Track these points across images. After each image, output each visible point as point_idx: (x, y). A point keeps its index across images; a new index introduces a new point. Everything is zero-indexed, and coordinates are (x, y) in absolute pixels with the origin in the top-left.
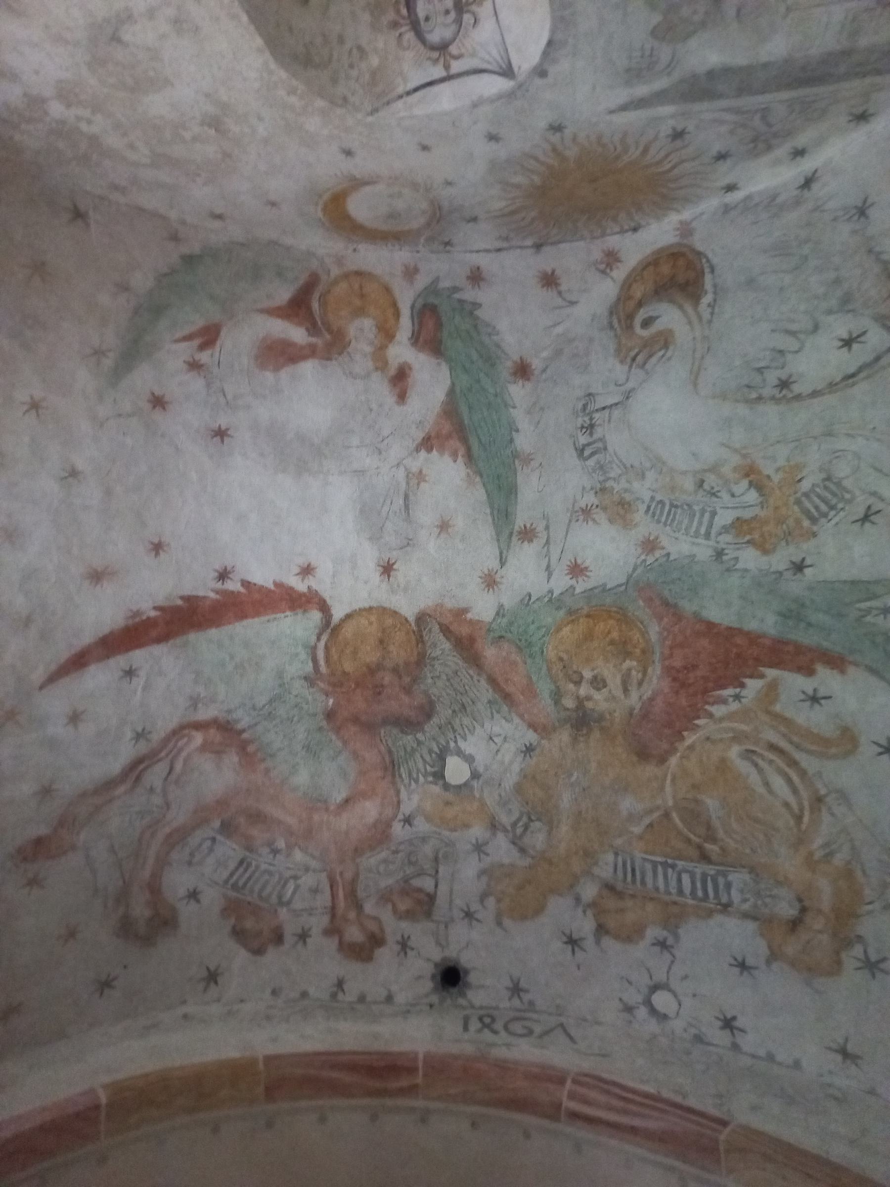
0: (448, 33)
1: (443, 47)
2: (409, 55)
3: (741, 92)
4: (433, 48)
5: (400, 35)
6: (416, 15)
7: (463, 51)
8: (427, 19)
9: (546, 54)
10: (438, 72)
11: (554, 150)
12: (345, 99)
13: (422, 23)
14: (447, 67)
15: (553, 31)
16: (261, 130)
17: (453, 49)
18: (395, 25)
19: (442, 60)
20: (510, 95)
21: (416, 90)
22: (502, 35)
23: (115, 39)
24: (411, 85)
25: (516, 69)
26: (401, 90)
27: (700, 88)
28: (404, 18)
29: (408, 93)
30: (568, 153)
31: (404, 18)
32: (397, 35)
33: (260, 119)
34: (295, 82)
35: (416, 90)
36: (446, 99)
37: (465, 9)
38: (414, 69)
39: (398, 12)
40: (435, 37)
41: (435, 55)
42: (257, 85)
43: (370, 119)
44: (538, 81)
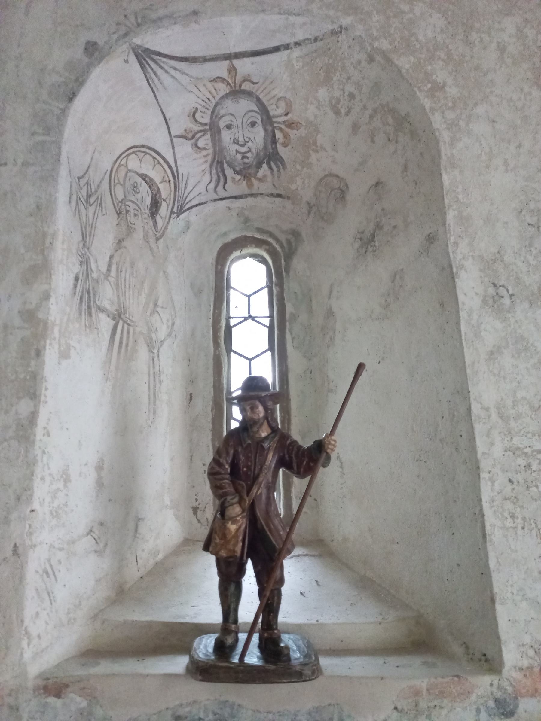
0: (229, 106)
1: (236, 93)
2: (278, 92)
4: (249, 94)
5: (286, 115)
6: (266, 130)
7: (209, 85)
8: (253, 124)
9: (80, 81)
10: (245, 66)
12: (371, 60)
13: (259, 121)
14: (232, 70)
15: (64, 112)
16: (510, 24)
17: (223, 89)
18: (291, 125)
19: (239, 78)
20: (143, 21)
21: (276, 49)
22: (157, 100)
24: (283, 55)
25: (132, 58)
26: (296, 53)
28: (281, 129)
29: (287, 47)
31: (281, 129)
32: (290, 115)
33: (502, 49)
34: (427, 103)
35: (276, 49)
36: (237, 31)
37: (207, 127)
38: (276, 75)
39: (286, 136)
40: (245, 105)
41: (246, 86)
42: (480, 110)
43: (347, 21)
44: (100, 38)
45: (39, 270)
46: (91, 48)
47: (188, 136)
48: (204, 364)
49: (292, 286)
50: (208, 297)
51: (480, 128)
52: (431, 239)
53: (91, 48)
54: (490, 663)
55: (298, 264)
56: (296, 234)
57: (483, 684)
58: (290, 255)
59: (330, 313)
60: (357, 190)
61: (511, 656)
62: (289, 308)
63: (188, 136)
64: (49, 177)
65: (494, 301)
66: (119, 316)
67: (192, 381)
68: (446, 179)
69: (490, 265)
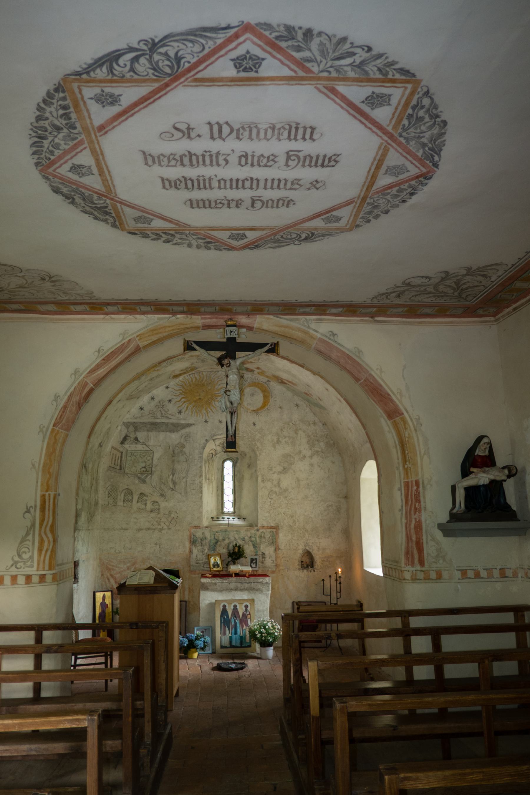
3: (167, 424)
9: (205, 446)
11: (208, 413)
23: (284, 469)
27: (176, 427)
30: (205, 412)
33: (268, 440)
44: (208, 439)
45: (201, 476)
46: (207, 440)
47: (219, 445)
48: (220, 484)
49: (236, 469)
50: (221, 471)
51: (264, 454)
52: (256, 471)
53: (207, 440)
54: (257, 526)
55: (238, 464)
56: (237, 458)
57: (256, 528)
58: (236, 463)
59: (243, 476)
60: (248, 456)
61: (259, 525)
62: (236, 473)
63: (219, 445)
64: (201, 462)
65: (263, 481)
66: (209, 479)
67: (217, 487)
68: (258, 462)
69: (263, 475)
